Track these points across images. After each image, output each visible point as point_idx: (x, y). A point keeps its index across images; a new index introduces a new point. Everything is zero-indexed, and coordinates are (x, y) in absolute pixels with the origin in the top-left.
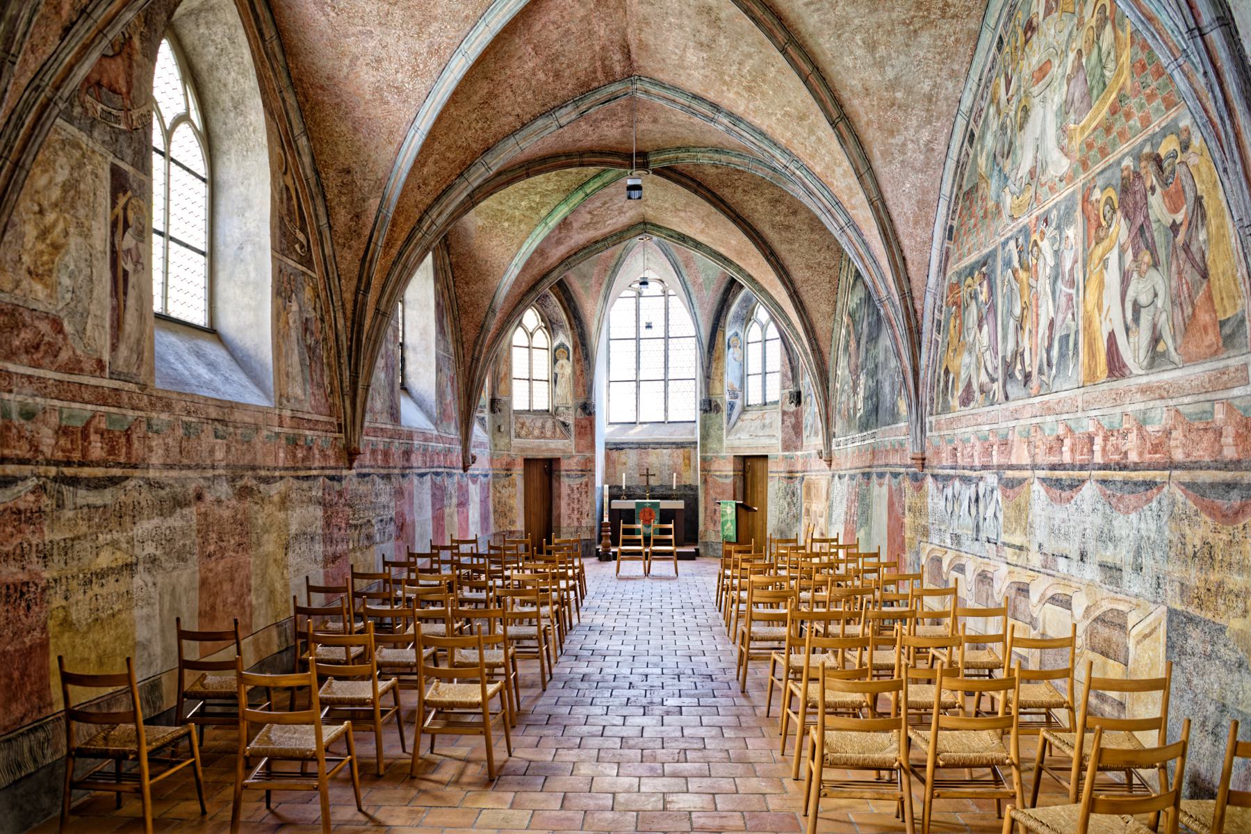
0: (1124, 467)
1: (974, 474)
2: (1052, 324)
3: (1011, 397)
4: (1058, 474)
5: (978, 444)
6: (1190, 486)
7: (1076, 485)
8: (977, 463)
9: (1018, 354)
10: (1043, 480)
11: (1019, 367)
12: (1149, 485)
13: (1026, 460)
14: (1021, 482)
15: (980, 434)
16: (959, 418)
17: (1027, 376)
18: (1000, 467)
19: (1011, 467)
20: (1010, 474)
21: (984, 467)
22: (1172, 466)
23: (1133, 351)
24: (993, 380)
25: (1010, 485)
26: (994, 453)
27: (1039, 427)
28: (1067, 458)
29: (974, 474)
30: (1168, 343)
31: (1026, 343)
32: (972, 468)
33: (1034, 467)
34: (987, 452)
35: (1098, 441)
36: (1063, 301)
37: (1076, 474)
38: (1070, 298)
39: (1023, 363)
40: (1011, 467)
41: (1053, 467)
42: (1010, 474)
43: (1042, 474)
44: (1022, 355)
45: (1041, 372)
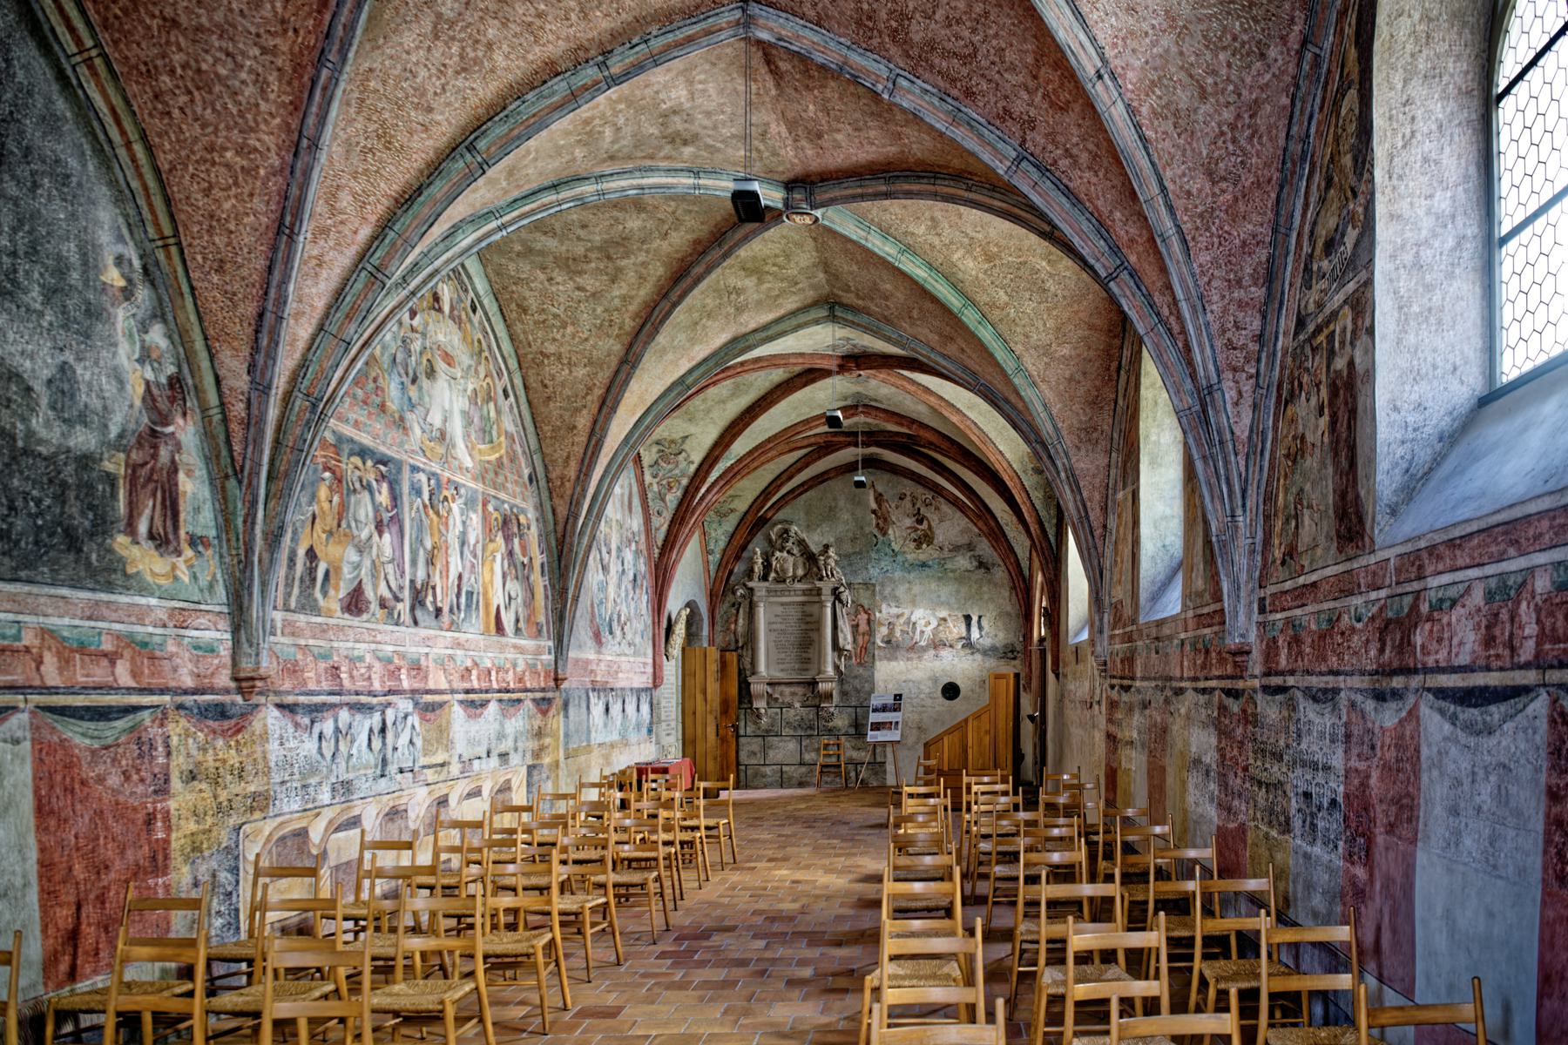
0: (508, 691)
1: (375, 701)
2: (460, 577)
3: (421, 623)
4: (472, 696)
5: (377, 666)
6: (534, 700)
7: (484, 704)
8: (377, 686)
9: (428, 585)
10: (461, 702)
11: (430, 598)
12: (519, 701)
13: (444, 685)
14: (441, 705)
15: (381, 654)
16: (341, 628)
17: (438, 611)
18: (414, 691)
19: (428, 692)
20: (429, 698)
21: (390, 692)
22: (526, 690)
23: (508, 620)
24: (397, 599)
25: (428, 710)
26: (403, 677)
27: (451, 657)
28: (476, 685)
29: (375, 701)
30: (522, 625)
31: (437, 580)
32: (371, 694)
33: (453, 692)
34: (394, 674)
35: (493, 673)
36: (468, 565)
37: (484, 696)
38: (473, 566)
39: (434, 595)
40: (428, 692)
41: (467, 692)
42: (429, 698)
43: (461, 697)
44: (434, 588)
45: (451, 611)
